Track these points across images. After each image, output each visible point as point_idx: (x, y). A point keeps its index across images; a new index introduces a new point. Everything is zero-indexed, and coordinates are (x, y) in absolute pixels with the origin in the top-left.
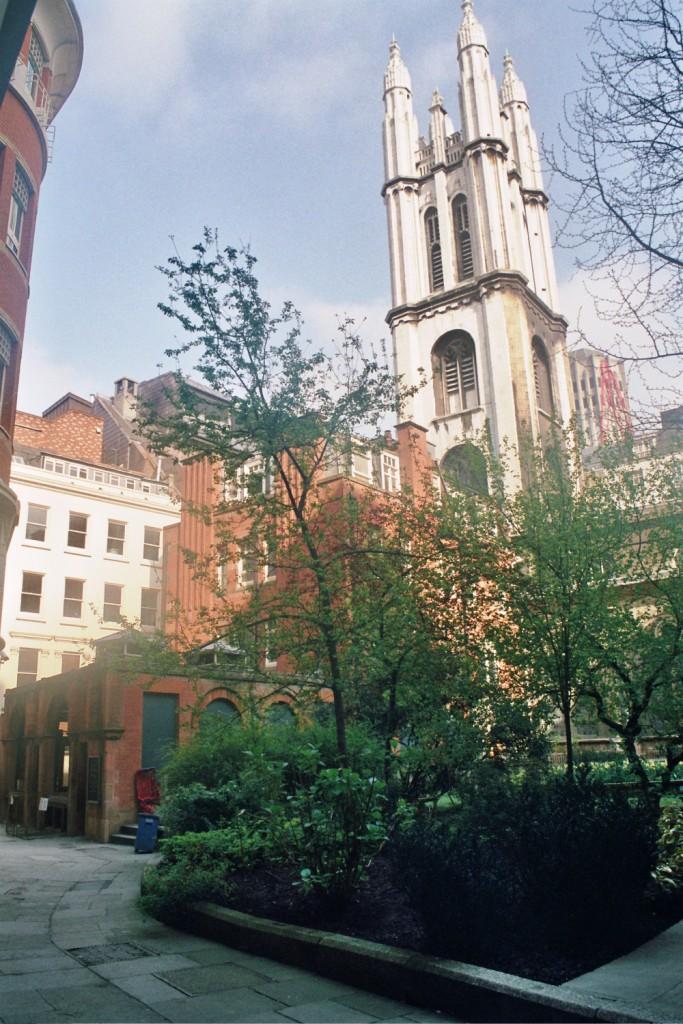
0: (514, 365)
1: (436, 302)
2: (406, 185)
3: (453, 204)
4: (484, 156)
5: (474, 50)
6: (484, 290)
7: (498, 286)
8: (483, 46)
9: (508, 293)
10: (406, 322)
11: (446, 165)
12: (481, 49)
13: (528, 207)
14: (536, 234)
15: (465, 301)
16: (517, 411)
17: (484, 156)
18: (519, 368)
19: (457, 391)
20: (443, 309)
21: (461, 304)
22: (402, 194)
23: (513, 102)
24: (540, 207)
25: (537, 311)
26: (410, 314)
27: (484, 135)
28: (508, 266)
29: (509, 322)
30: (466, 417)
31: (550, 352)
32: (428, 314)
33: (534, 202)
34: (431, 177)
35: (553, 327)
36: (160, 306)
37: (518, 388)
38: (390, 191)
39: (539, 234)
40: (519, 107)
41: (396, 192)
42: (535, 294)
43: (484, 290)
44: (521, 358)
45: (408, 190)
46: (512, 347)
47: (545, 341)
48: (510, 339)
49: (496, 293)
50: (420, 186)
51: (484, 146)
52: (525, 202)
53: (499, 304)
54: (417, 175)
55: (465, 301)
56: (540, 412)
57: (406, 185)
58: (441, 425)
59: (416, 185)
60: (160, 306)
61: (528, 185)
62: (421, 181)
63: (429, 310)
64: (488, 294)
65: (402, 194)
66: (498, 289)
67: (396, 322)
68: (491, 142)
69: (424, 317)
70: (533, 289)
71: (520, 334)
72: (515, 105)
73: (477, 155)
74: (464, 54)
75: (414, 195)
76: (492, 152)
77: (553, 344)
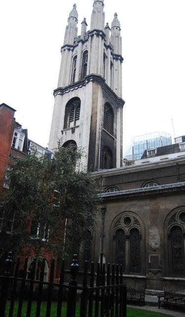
0: (93, 109)
1: (70, 87)
4: (95, 36)
7: (92, 80)
11: (84, 40)
17: (95, 36)
26: (60, 92)
27: (96, 29)
28: (97, 72)
29: (93, 93)
30: (73, 131)
32: (67, 92)
33: (117, 59)
38: (63, 49)
41: (65, 50)
43: (87, 81)
44: (97, 107)
47: (112, 106)
52: (114, 59)
53: (90, 86)
58: (64, 132)
59: (72, 48)
64: (87, 83)
68: (98, 31)
70: (109, 85)
71: (97, 98)
73: (92, 36)
75: (71, 51)
76: (98, 35)
77: (117, 108)
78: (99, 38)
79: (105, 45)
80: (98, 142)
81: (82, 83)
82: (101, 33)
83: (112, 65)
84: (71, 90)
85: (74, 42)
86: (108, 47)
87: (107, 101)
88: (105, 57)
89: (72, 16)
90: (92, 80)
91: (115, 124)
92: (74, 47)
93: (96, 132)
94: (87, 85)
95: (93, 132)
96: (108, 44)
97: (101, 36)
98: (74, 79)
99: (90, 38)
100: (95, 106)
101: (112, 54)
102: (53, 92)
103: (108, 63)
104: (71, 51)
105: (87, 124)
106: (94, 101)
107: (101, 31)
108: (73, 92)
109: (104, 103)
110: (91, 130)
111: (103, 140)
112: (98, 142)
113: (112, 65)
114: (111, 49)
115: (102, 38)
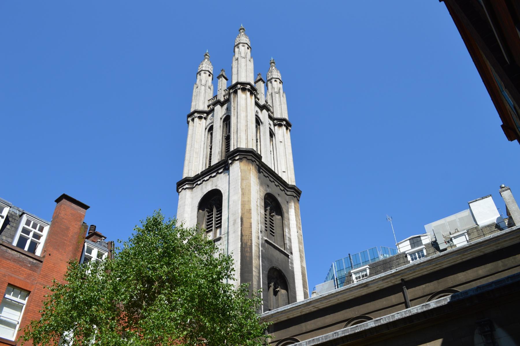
0: (243, 205)
2: (198, 115)
3: (224, 122)
4: (239, 92)
5: (241, 45)
6: (230, 162)
7: (237, 158)
8: (247, 44)
9: (244, 161)
10: (185, 189)
12: (246, 45)
13: (276, 127)
14: (281, 142)
15: (220, 171)
16: (242, 235)
18: (247, 207)
19: (212, 230)
20: (208, 177)
21: (218, 173)
22: (196, 120)
23: (272, 79)
24: (284, 128)
25: (272, 180)
29: (242, 179)
31: (283, 206)
32: (199, 183)
33: (280, 125)
34: (212, 110)
35: (288, 193)
36: (86, 207)
37: (244, 219)
38: (190, 119)
39: (283, 142)
40: (276, 81)
41: (193, 120)
42: (274, 172)
43: (230, 162)
44: (249, 201)
45: (200, 118)
46: (243, 194)
48: (242, 189)
49: (237, 162)
50: (208, 115)
51: (239, 86)
52: (275, 125)
54: (206, 109)
55: (220, 171)
56: (266, 240)
57: (198, 115)
59: (205, 115)
60: (86, 207)
61: (277, 115)
62: (208, 113)
63: (200, 180)
64: (231, 163)
65: (196, 120)
66: (237, 160)
67: (180, 190)
69: (197, 184)
72: (273, 80)
73: (236, 92)
74: (269, 82)
75: (203, 120)
76: (244, 90)
78: (246, 94)
79: (257, 104)
80: (257, 263)
81: (224, 166)
82: (248, 87)
83: (272, 134)
84: (206, 179)
85: (209, 106)
86: (262, 108)
87: (269, 191)
88: (258, 122)
89: (204, 69)
90: (237, 158)
91: (286, 230)
92: (208, 113)
93: (251, 243)
94: (231, 168)
95: (246, 244)
96: (262, 102)
97: (249, 90)
98: (210, 159)
99: (232, 96)
100: (246, 199)
101: (270, 117)
102: (176, 186)
103: (265, 132)
104: (203, 120)
105: (234, 232)
106: (245, 192)
107: (249, 84)
108: (209, 183)
109: (263, 195)
110: (241, 241)
111: (265, 257)
112: (257, 263)
113: (272, 134)
114: (268, 110)
115: (251, 94)
